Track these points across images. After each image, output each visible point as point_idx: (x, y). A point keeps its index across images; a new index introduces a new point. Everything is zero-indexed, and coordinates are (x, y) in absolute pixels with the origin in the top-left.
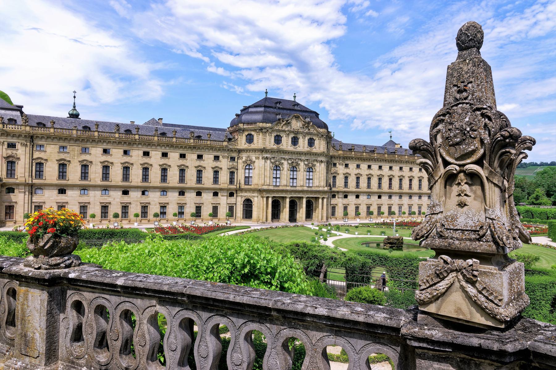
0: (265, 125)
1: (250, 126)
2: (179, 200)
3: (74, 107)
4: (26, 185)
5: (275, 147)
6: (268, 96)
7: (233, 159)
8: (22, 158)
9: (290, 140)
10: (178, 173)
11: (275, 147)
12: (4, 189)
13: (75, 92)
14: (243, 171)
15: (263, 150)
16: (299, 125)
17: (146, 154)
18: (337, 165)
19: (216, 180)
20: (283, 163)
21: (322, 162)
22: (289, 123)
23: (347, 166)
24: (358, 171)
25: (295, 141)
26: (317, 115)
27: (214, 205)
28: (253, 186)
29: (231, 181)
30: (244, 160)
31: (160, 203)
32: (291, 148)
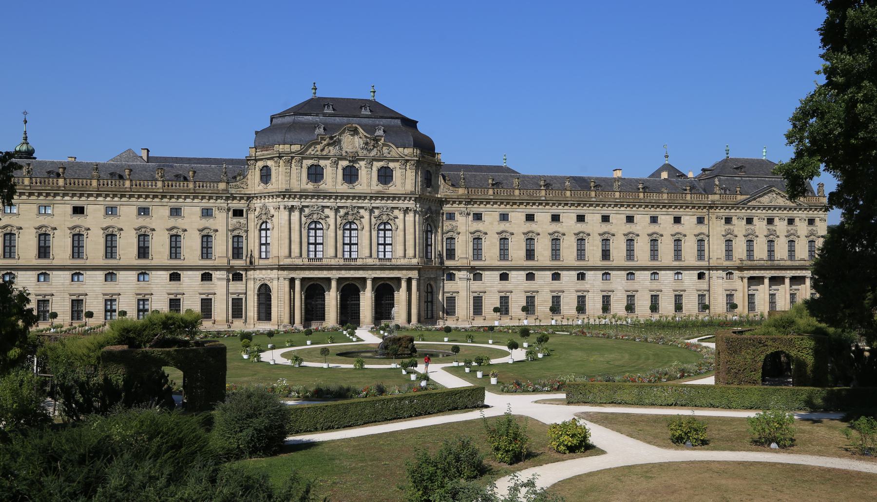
0: (287, 148)
1: (265, 152)
3: (26, 139)
6: (318, 95)
7: (238, 213)
10: (135, 241)
11: (310, 186)
13: (25, 113)
14: (257, 232)
15: (286, 194)
17: (78, 210)
18: (457, 216)
19: (206, 250)
20: (328, 217)
21: (406, 211)
22: (335, 142)
23: (478, 217)
24: (504, 226)
25: (350, 175)
26: (411, 124)
27: (204, 297)
28: (270, 260)
29: (237, 253)
30: (257, 213)
31: (104, 295)
32: (343, 188)
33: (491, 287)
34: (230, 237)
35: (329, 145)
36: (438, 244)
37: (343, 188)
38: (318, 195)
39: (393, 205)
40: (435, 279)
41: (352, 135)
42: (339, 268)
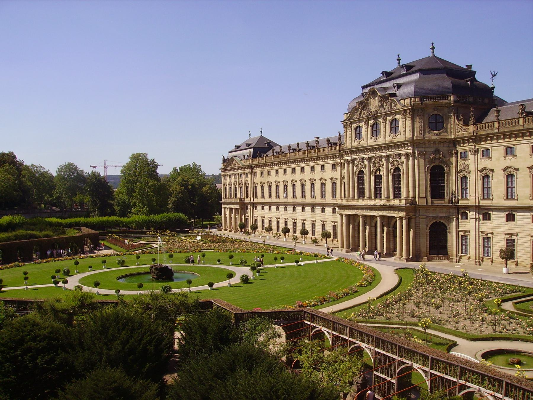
2: (313, 217)
8: (249, 183)
9: (370, 128)
21: (407, 156)
23: (486, 154)
24: (510, 162)
25: (375, 131)
32: (371, 142)
33: (499, 228)
35: (363, 109)
36: (452, 183)
39: (399, 152)
41: (374, 98)
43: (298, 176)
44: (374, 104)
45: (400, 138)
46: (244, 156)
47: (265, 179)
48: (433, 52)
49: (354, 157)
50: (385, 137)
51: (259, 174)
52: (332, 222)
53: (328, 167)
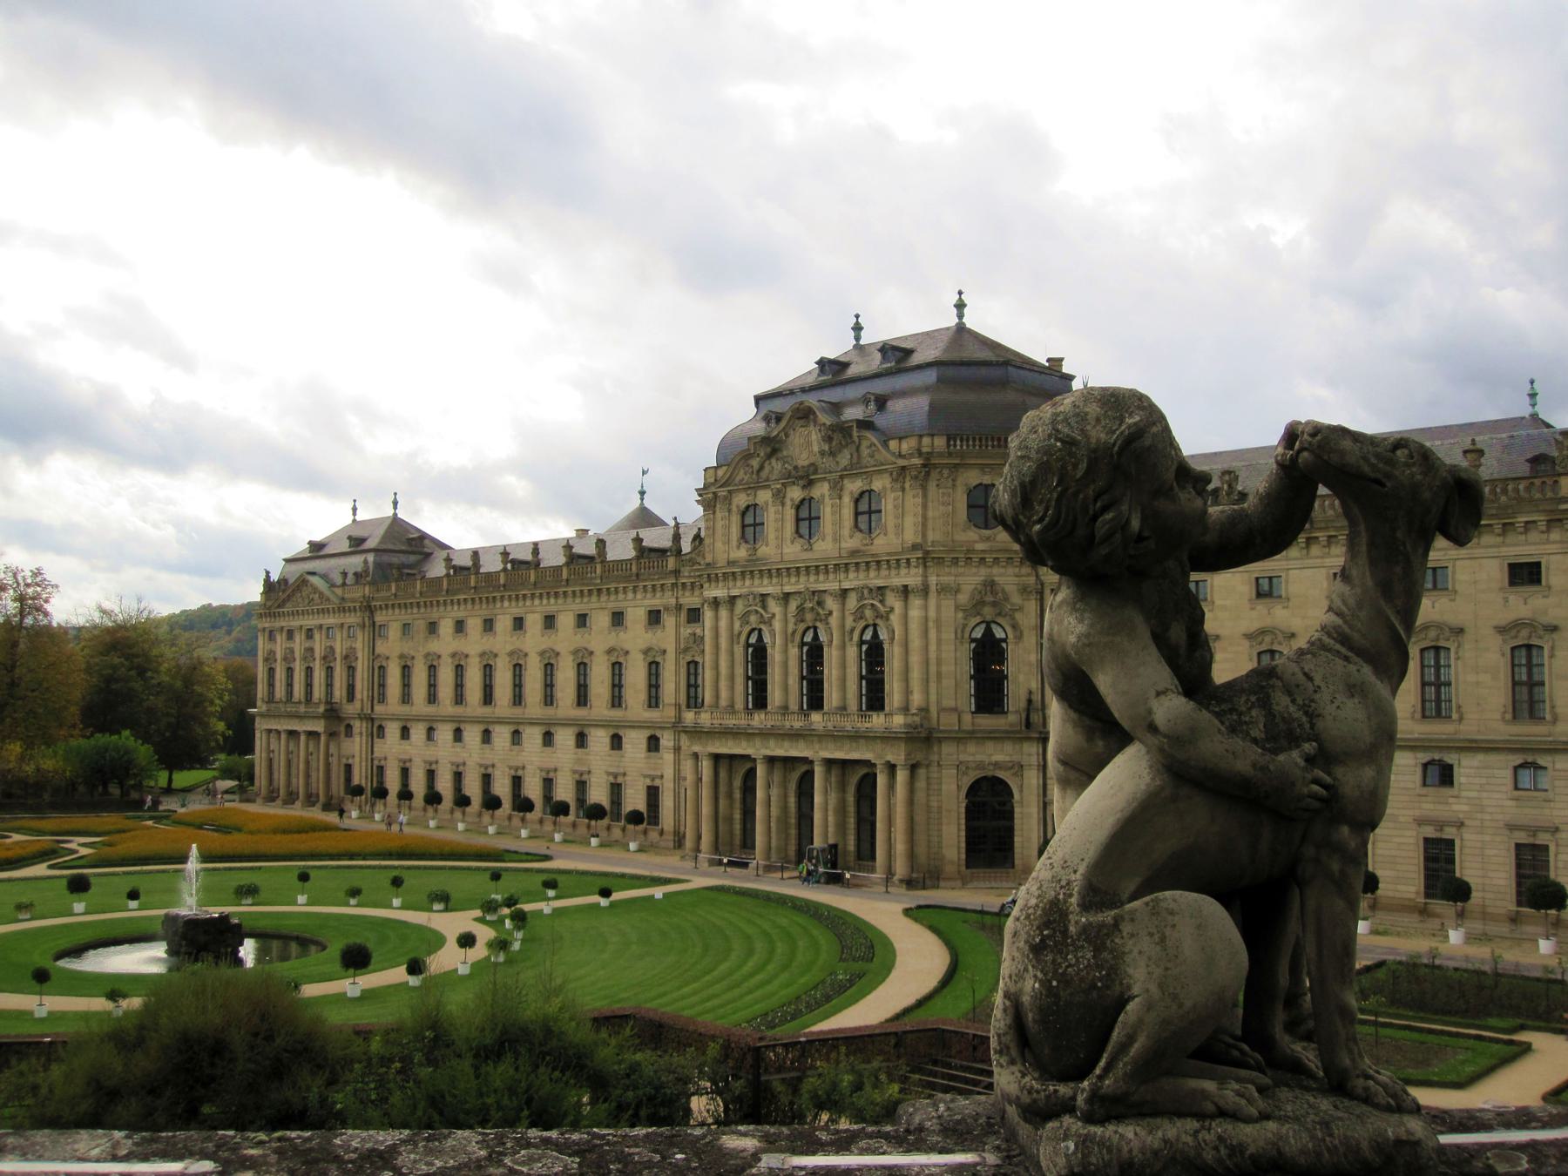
2: (578, 761)
4: (363, 717)
5: (742, 553)
8: (360, 655)
9: (790, 513)
11: (742, 553)
12: (342, 729)
16: (816, 449)
21: (905, 591)
25: (806, 519)
32: (793, 551)
34: (683, 663)
37: (793, 551)
38: (753, 569)
39: (880, 583)
40: (1019, 768)
42: (765, 734)
43: (534, 640)
44: (806, 445)
45: (883, 544)
46: (345, 574)
47: (419, 648)
48: (960, 316)
49: (735, 592)
50: (837, 539)
51: (394, 631)
52: (645, 776)
53: (636, 615)
